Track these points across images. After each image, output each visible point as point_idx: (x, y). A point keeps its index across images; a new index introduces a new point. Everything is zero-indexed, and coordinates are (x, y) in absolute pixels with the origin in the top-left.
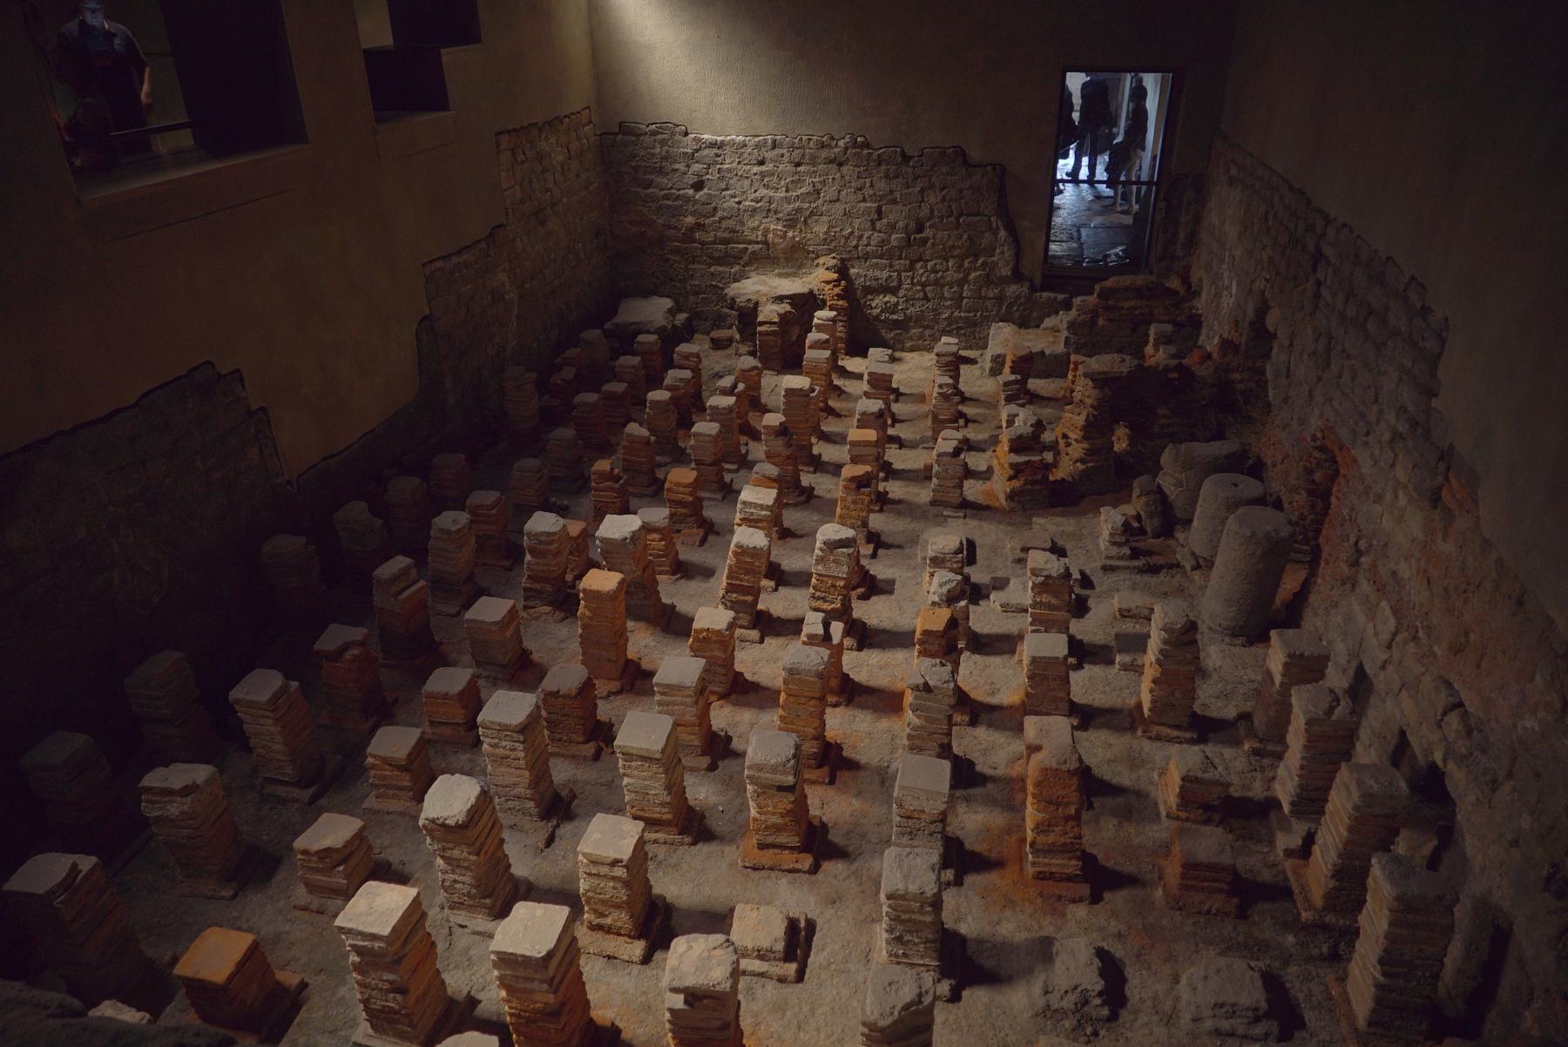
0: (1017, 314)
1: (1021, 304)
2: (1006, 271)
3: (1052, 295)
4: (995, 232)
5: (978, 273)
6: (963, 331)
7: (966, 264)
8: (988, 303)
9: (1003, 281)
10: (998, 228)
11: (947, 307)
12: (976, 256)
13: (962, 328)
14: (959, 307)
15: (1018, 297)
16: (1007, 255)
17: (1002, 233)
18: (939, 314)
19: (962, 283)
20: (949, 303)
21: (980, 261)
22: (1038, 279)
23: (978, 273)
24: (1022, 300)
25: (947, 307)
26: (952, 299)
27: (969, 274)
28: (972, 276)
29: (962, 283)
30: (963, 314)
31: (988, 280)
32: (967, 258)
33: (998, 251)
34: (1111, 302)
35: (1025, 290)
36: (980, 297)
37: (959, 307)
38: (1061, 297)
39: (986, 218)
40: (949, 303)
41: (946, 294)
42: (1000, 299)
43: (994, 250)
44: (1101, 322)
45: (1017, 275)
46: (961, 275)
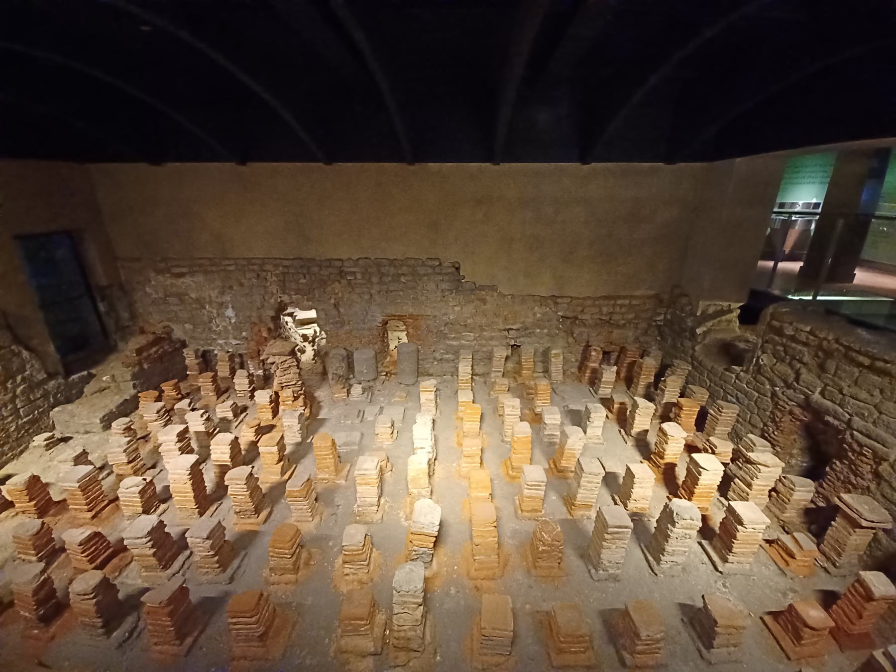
0: (62, 398)
1: (62, 391)
2: (42, 376)
3: (79, 375)
4: (19, 354)
5: (22, 387)
6: (31, 431)
7: (9, 385)
8: (38, 402)
9: (44, 382)
10: (20, 352)
11: (11, 422)
12: (14, 378)
13: (29, 429)
14: (19, 417)
15: (58, 387)
16: (36, 366)
17: (25, 354)
18: (8, 430)
19: (13, 400)
20: (10, 419)
21: (19, 378)
22: (61, 369)
23: (22, 387)
24: (62, 388)
25: (11, 422)
26: (11, 415)
27: (15, 392)
28: (18, 391)
29: (13, 400)
30: (25, 420)
31: (32, 386)
32: (7, 382)
33: (28, 366)
34: (145, 354)
35: (61, 380)
36: (31, 402)
37: (19, 417)
38: (85, 373)
39: (8, 349)
40: (10, 419)
41: (5, 414)
42: (45, 396)
43: (25, 366)
44: (146, 366)
45: (51, 376)
46: (11, 395)
